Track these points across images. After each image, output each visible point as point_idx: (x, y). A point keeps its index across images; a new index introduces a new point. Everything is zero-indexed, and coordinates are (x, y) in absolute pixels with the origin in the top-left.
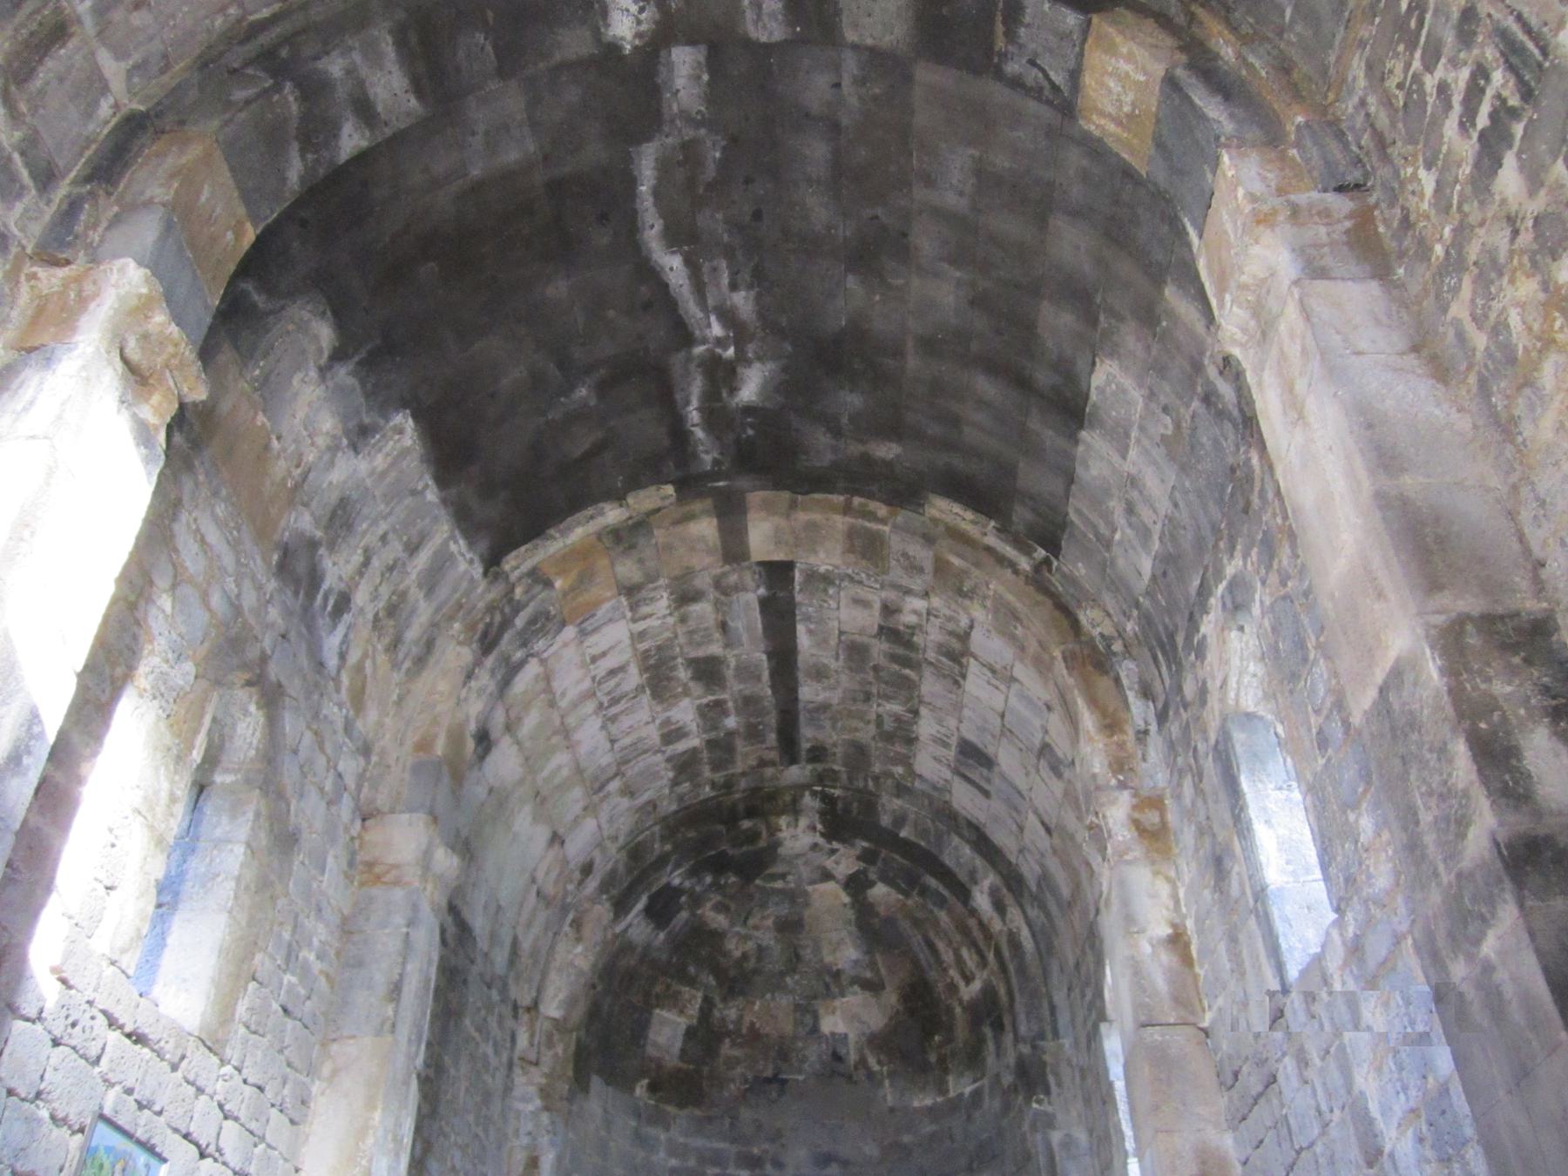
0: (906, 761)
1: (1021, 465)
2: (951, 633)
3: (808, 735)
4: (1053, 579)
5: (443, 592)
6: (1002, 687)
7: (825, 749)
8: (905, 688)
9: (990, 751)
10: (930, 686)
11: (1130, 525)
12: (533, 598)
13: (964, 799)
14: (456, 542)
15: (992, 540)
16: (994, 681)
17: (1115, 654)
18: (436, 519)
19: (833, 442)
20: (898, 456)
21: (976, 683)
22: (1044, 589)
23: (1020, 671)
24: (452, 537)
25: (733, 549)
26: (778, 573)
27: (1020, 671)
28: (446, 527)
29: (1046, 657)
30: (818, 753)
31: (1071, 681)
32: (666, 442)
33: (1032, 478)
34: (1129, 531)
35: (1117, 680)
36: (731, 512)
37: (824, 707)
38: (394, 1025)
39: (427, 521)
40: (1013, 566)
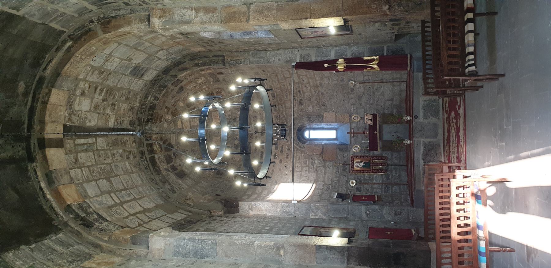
0: (136, 95)
1: (31, 39)
2: (93, 73)
3: (126, 125)
4: (76, 34)
5: (71, 241)
6: (113, 58)
7: (131, 121)
8: (110, 91)
9: (134, 65)
10: (111, 82)
11: (58, 4)
12: (74, 211)
13: (149, 76)
14: (51, 237)
15: (60, 54)
16: (110, 61)
17: (104, 16)
18: (43, 244)
19: (17, 106)
20: (25, 83)
21: (111, 66)
22: (80, 38)
23: (107, 51)
24: (50, 238)
25: (59, 144)
26: (67, 129)
27: (107, 51)
28: (46, 241)
29: (104, 40)
30: (132, 123)
31: (113, 33)
32: (14, 166)
33: (37, 35)
34: (60, 5)
35: (113, 17)
36: (43, 144)
37: (116, 120)
38: (214, 240)
39: (43, 247)
40: (70, 47)
